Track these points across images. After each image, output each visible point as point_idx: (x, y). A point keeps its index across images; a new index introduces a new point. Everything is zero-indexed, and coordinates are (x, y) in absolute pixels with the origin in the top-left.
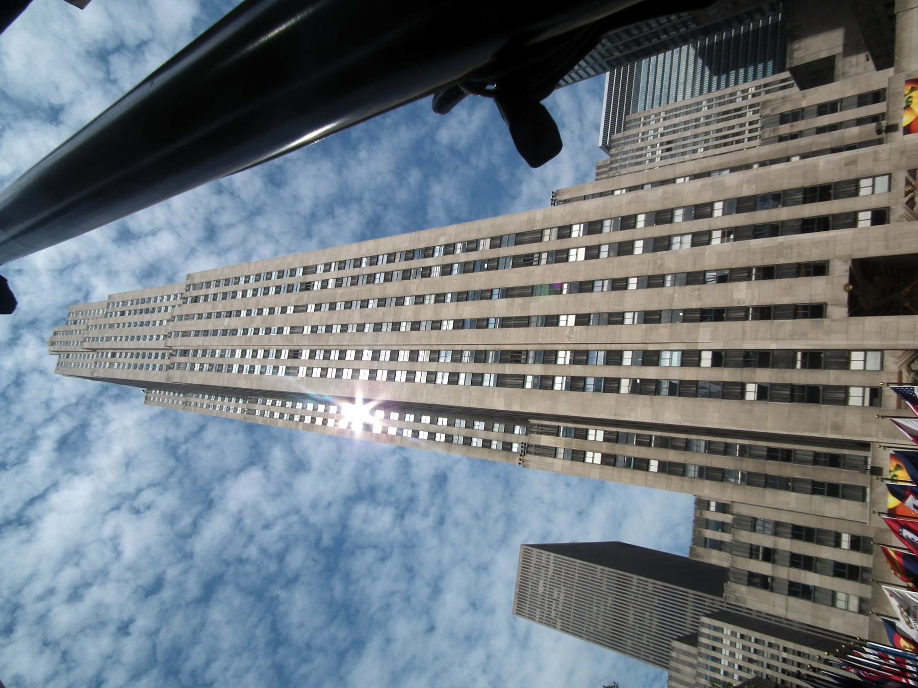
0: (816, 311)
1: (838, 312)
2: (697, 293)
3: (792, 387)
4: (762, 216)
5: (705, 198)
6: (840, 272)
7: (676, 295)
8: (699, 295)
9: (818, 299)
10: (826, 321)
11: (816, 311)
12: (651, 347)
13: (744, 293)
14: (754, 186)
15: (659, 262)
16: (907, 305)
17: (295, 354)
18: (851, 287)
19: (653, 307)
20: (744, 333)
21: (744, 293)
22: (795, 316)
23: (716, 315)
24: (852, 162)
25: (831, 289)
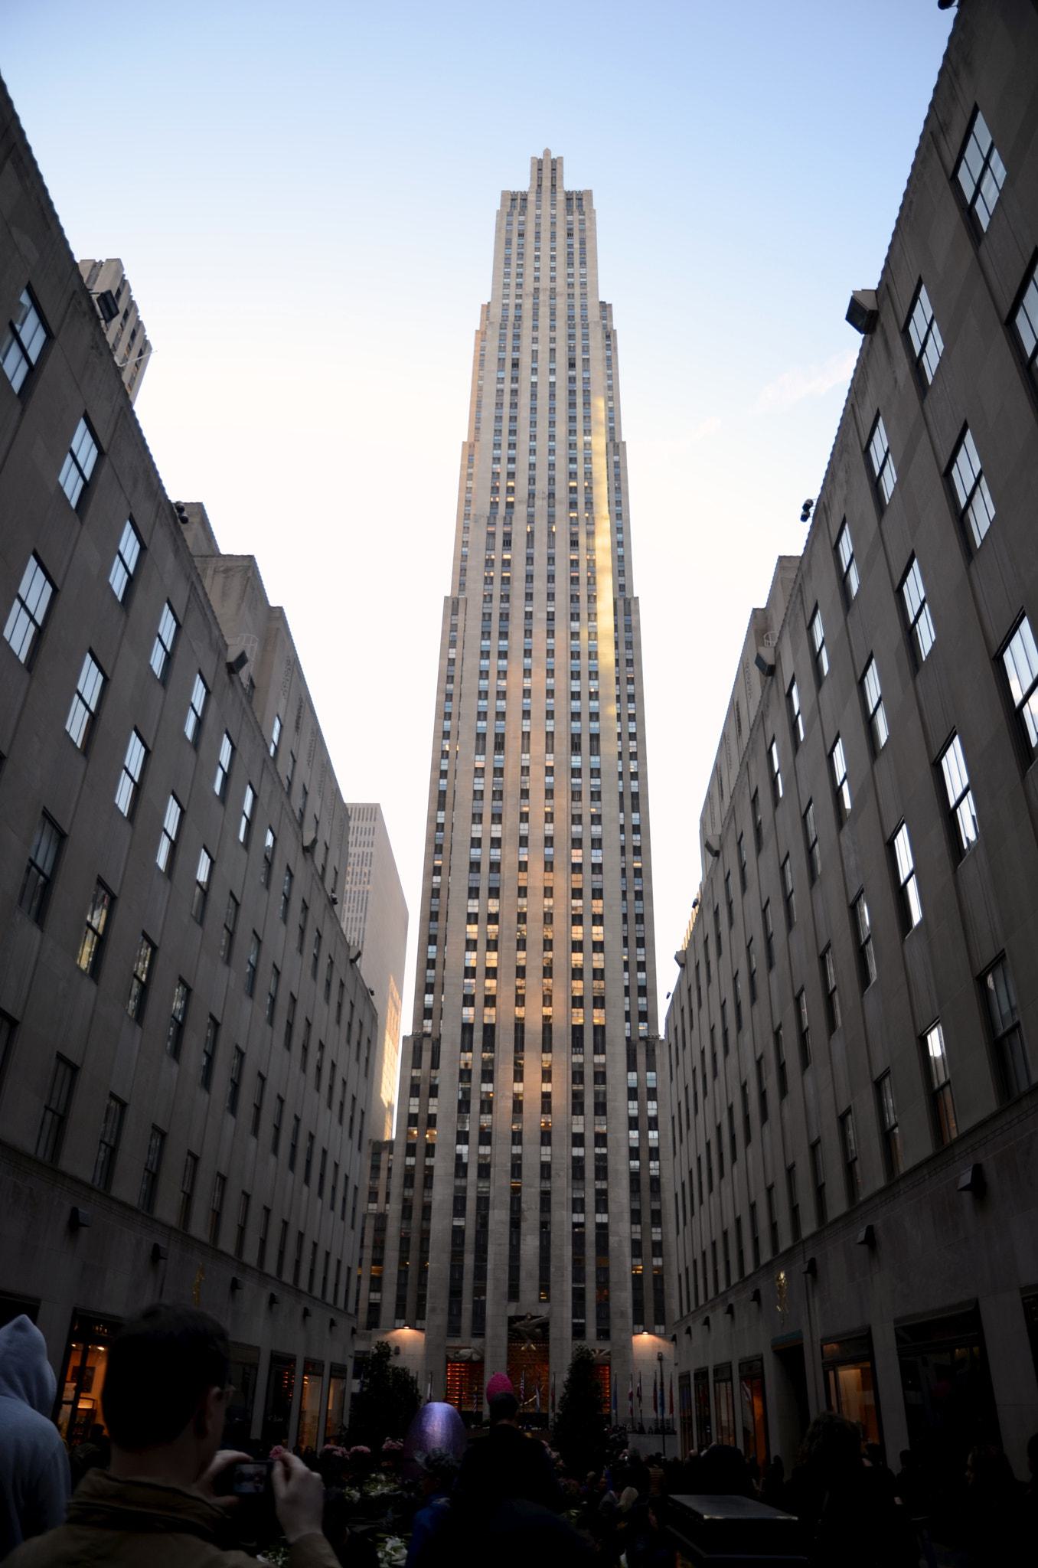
0: (514, 1294)
1: (512, 1310)
3: (461, 1278)
4: (590, 1252)
5: (611, 1206)
6: (543, 1311)
9: (522, 1296)
10: (505, 1302)
11: (514, 1294)
13: (530, 1244)
19: (525, 1171)
21: (530, 1244)
22: (511, 1279)
23: (515, 1224)
24: (623, 1314)
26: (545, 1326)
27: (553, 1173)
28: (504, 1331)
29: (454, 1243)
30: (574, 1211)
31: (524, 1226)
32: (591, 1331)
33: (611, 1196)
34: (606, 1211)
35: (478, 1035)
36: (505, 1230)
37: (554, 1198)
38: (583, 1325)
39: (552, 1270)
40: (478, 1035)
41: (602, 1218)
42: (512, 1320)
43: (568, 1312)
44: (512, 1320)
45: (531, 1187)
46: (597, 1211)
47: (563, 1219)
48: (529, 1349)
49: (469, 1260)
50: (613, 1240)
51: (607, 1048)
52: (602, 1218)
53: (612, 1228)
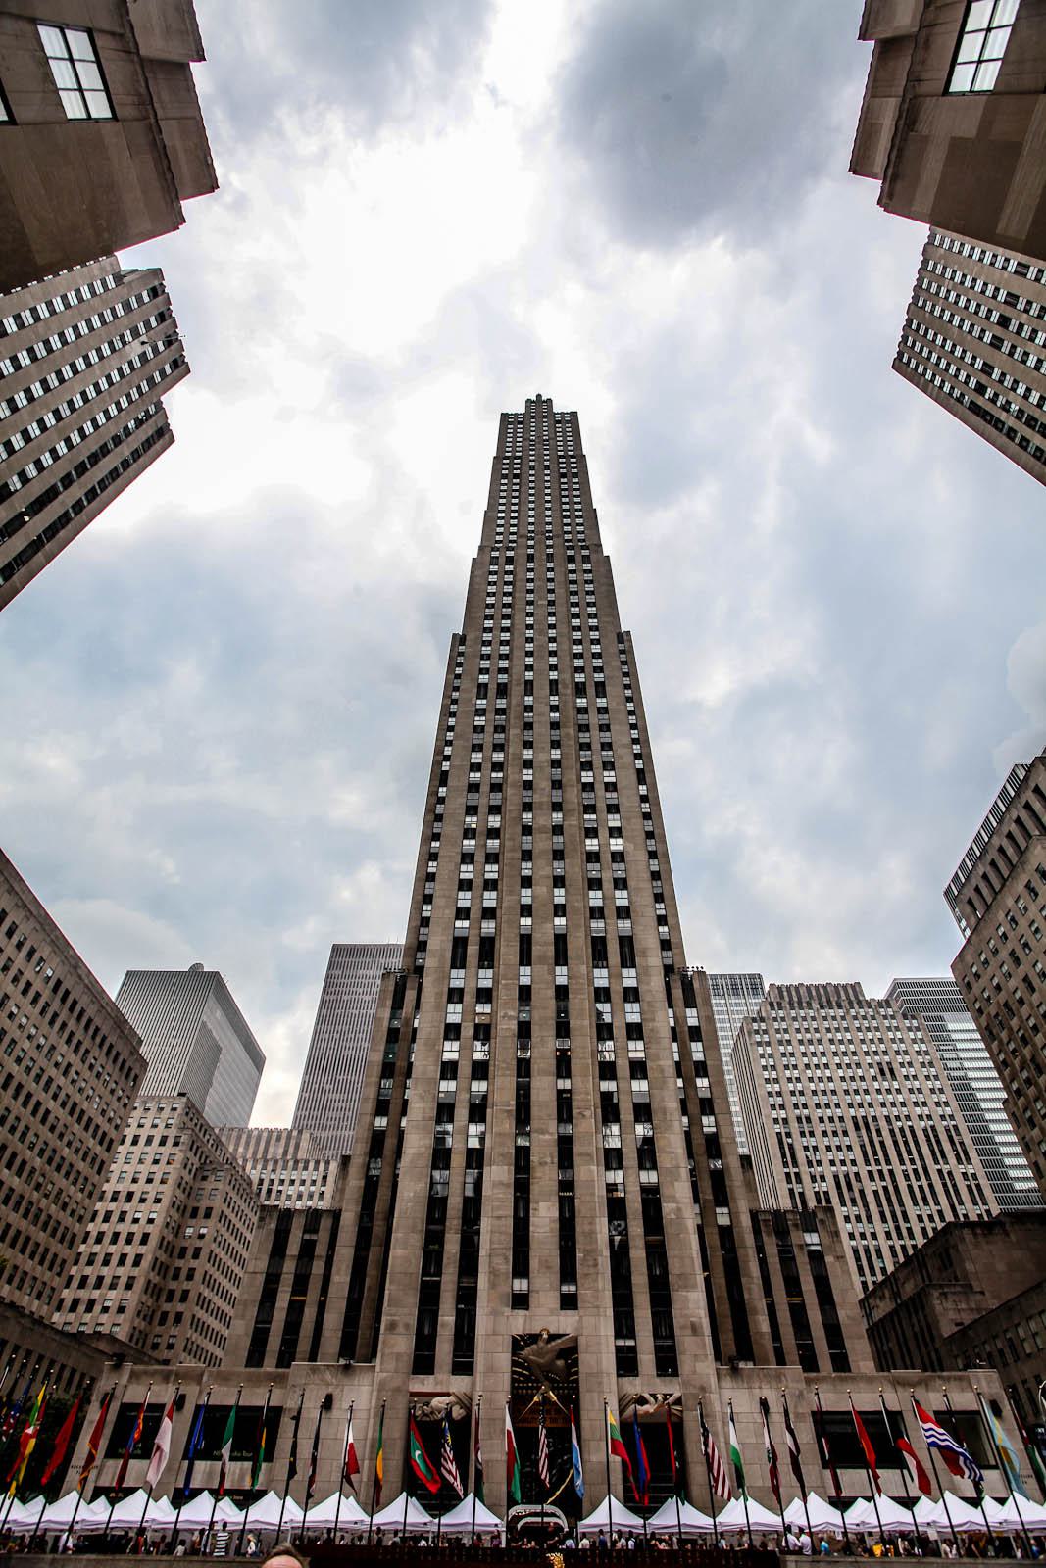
1: (519, 1323)
2: (549, 1160)
5: (662, 1160)
6: (566, 1323)
7: (547, 1137)
8: (546, 1163)
12: (489, 1111)
13: (544, 1216)
14: (673, 1216)
15: (587, 1113)
16: (536, 1399)
17: (503, 690)
18: (545, 1336)
20: (499, 1218)
21: (544, 1216)
23: (522, 1189)
25: (547, 1317)
26: (570, 1352)
27: (575, 1112)
28: (504, 1359)
29: (430, 1220)
30: (608, 1168)
31: (535, 1189)
32: (647, 1359)
33: (659, 1144)
34: (654, 1167)
35: (473, 950)
36: (508, 1195)
37: (577, 1148)
38: (633, 1349)
39: (579, 1255)
40: (473, 950)
41: (649, 1177)
42: (518, 1344)
43: (607, 1327)
44: (518, 1344)
45: (543, 1132)
46: (641, 1167)
47: (592, 1177)
48: (546, 1399)
49: (452, 1244)
50: (667, 1208)
51: (638, 960)
52: (649, 1177)
53: (665, 1191)
